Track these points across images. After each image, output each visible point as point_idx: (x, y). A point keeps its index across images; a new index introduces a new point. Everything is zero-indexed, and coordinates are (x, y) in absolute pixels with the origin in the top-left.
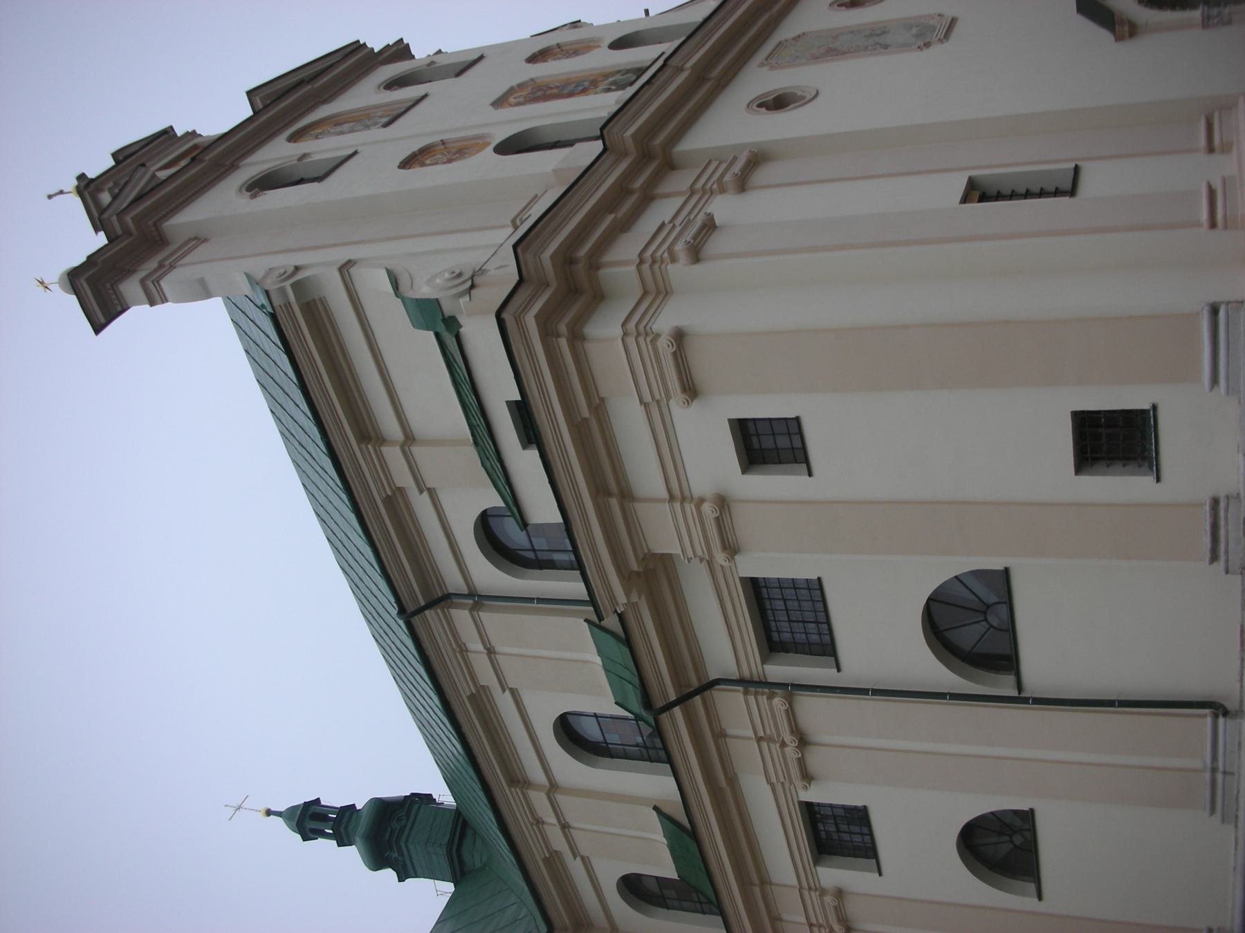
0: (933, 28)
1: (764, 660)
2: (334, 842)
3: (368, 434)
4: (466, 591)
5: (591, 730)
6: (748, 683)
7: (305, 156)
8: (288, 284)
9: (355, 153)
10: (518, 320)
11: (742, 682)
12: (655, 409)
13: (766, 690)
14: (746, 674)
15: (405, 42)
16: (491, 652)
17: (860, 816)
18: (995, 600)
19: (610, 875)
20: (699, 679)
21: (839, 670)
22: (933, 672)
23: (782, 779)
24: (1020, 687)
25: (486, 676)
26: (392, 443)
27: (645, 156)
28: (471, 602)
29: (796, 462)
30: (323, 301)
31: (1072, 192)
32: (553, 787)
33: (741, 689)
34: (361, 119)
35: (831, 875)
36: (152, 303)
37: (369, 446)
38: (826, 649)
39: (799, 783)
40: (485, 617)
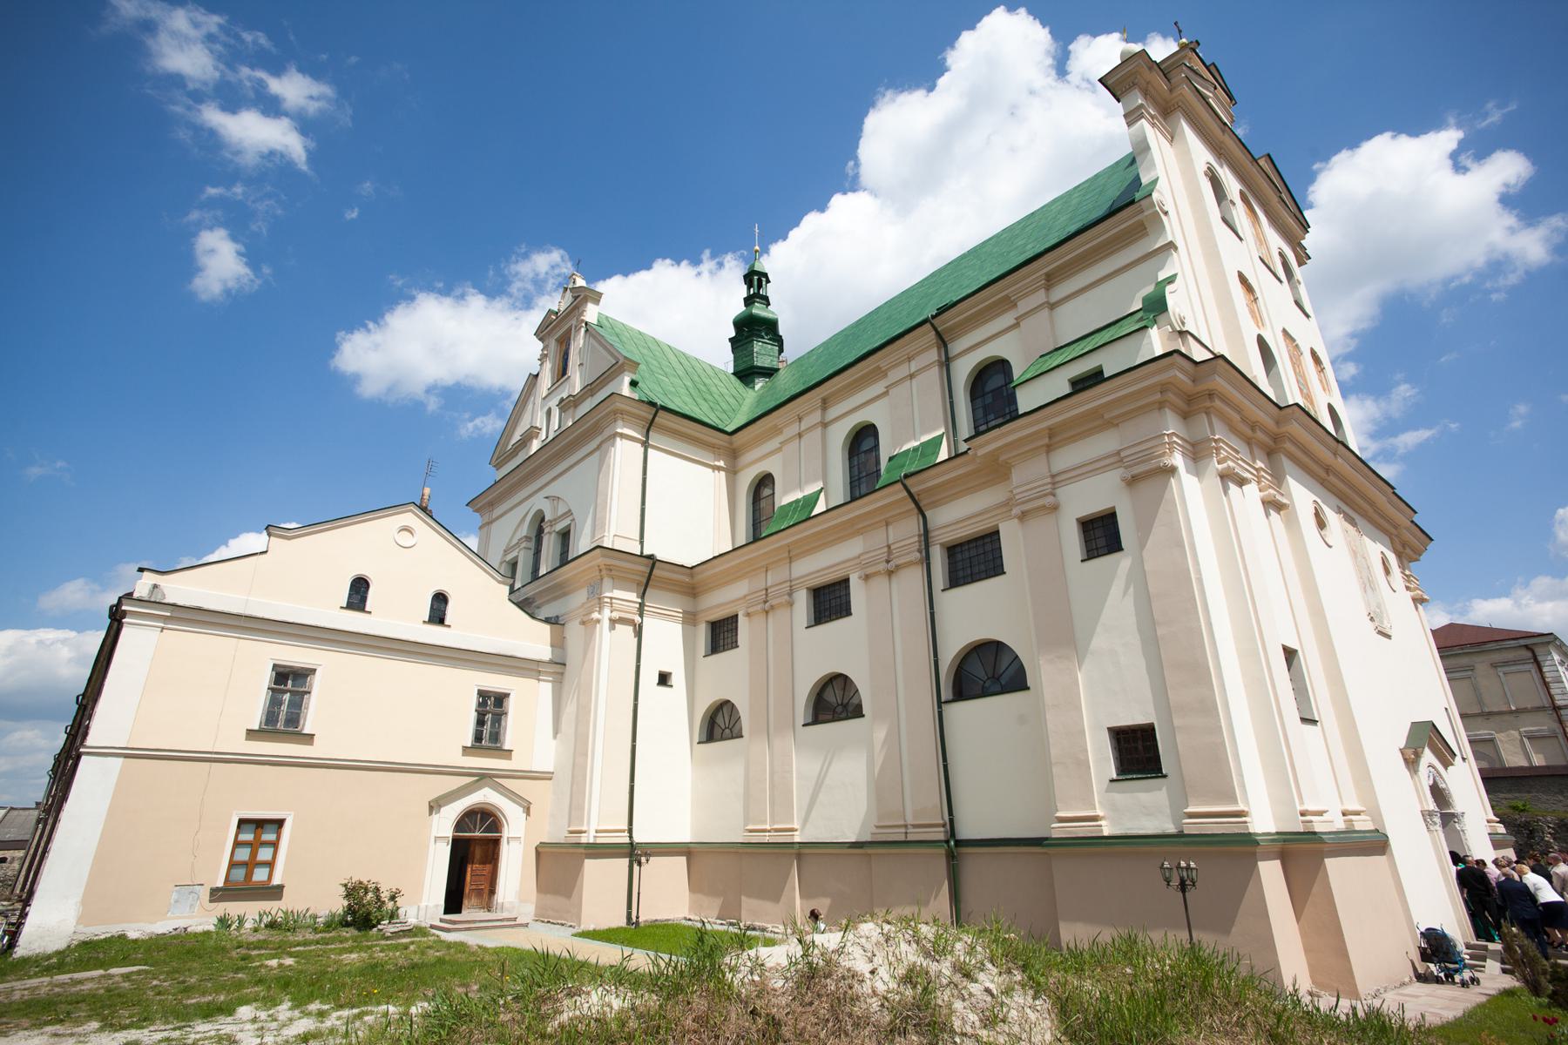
0: (1382, 622)
1: (942, 545)
2: (746, 296)
3: (1051, 280)
4: (951, 355)
5: (867, 444)
6: (926, 536)
7: (1234, 204)
8: (1158, 209)
9: (1241, 239)
10: (1172, 365)
11: (926, 532)
12: (1117, 459)
13: (923, 547)
14: (932, 534)
15: (1308, 261)
16: (912, 376)
17: (843, 610)
18: (1003, 683)
19: (772, 466)
20: (925, 506)
21: (943, 590)
22: (952, 648)
23: (863, 562)
24: (946, 702)
25: (894, 375)
26: (1047, 297)
27: (1276, 438)
28: (944, 359)
29: (1088, 551)
30: (1146, 234)
31: (1304, 720)
32: (825, 425)
33: (922, 532)
34: (1261, 240)
35: (802, 602)
36: (1125, 116)
37: (1043, 282)
38: (955, 580)
39: (862, 573)
40: (936, 369)
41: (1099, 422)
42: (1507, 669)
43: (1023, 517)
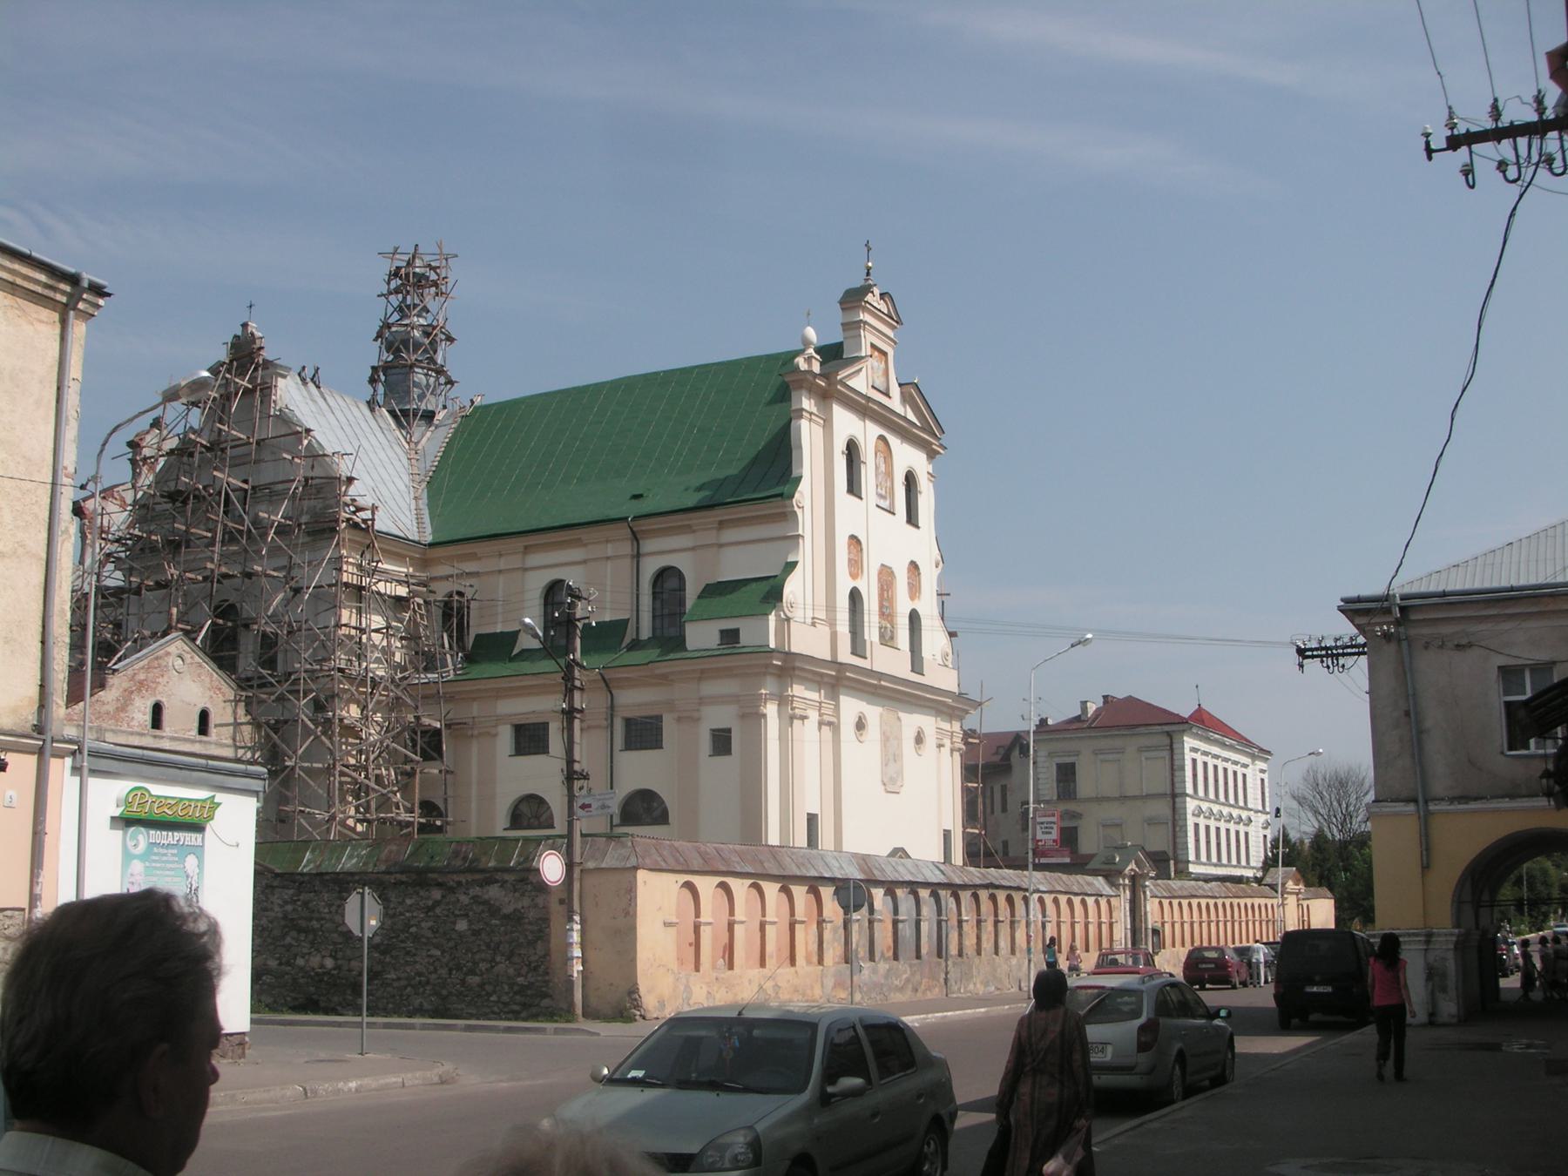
11: (612, 707)
24: (616, 826)
38: (630, 745)
40: (627, 562)
41: (728, 673)
42: (1147, 754)
43: (679, 720)
